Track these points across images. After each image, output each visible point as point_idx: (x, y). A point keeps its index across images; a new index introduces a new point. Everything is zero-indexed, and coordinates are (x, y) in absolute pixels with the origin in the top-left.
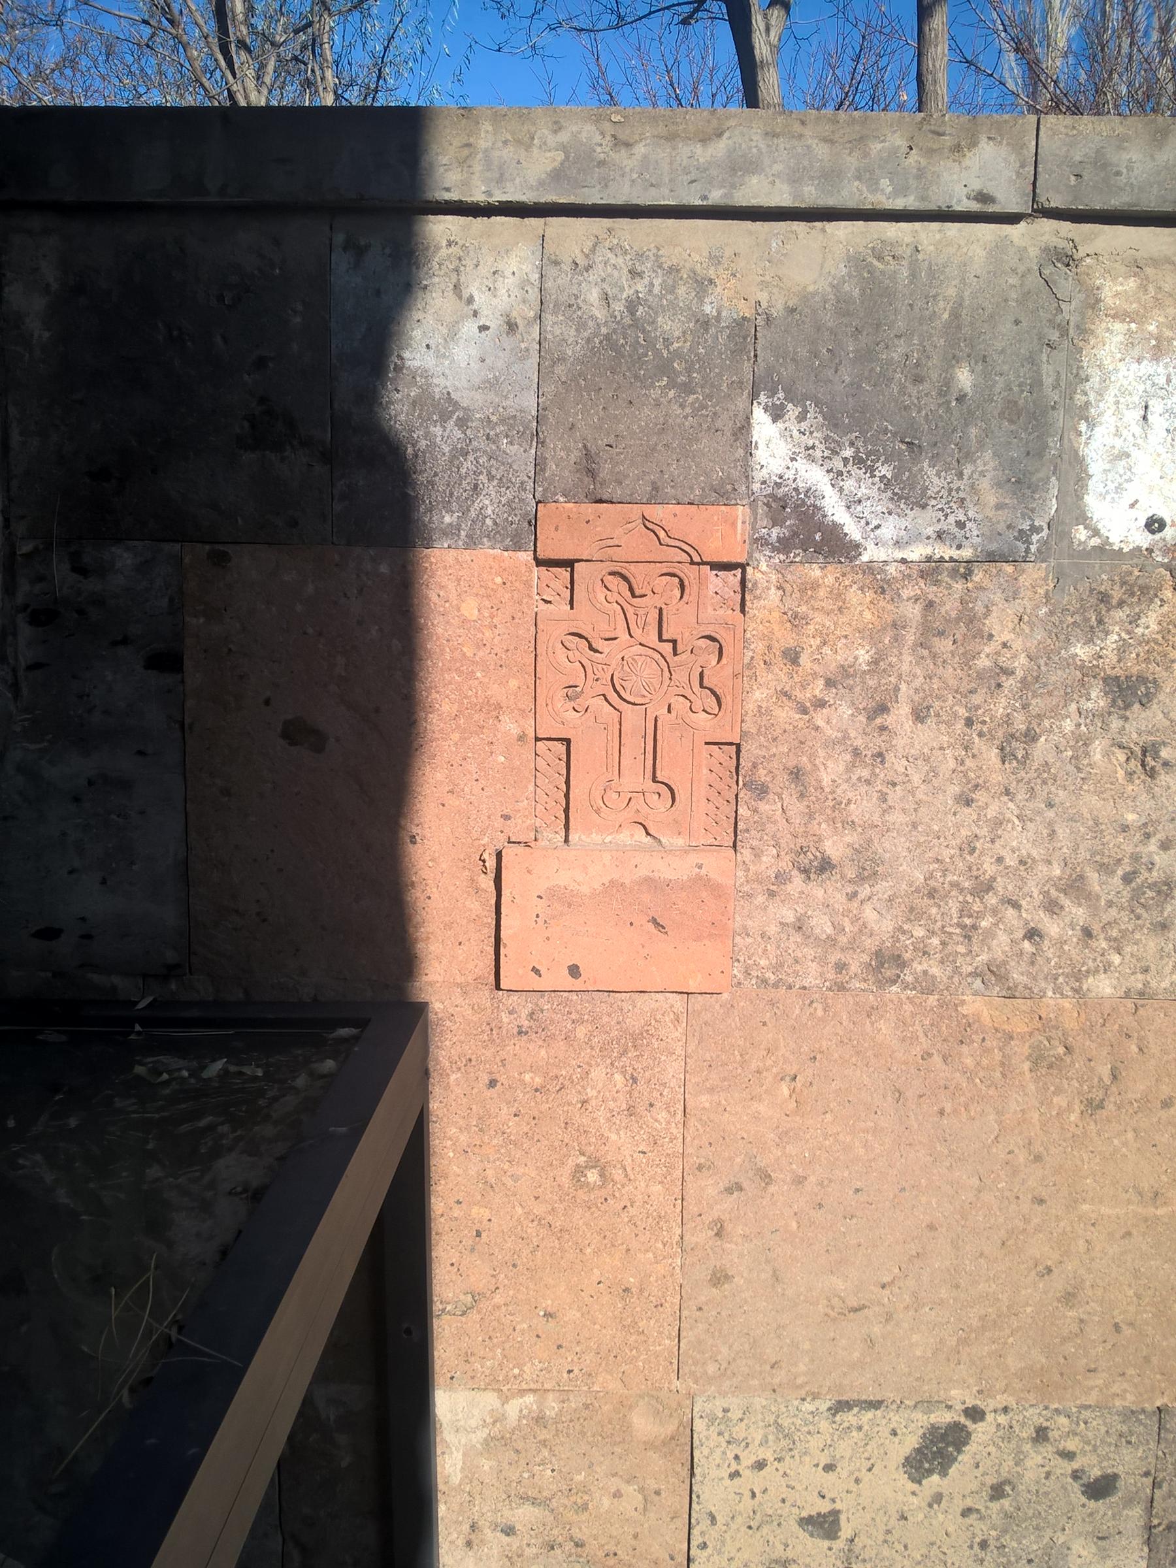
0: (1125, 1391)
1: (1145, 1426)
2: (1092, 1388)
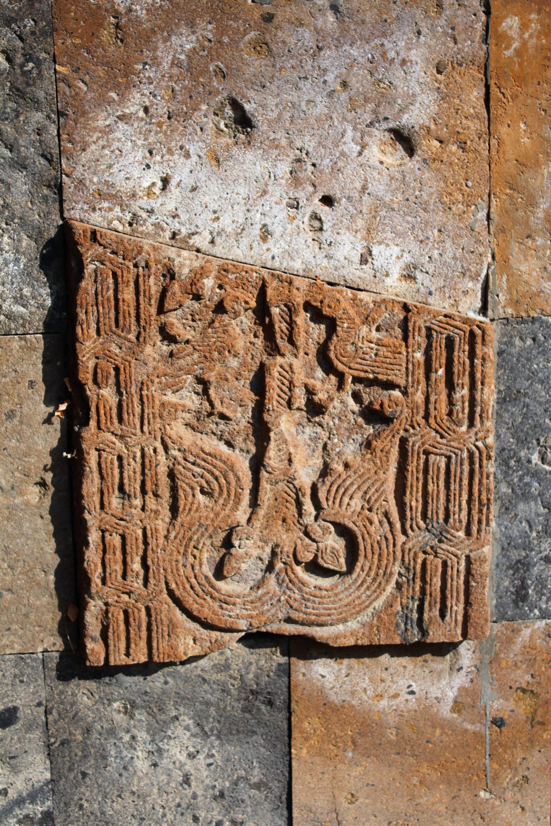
0: (12, 642)
1: (33, 668)
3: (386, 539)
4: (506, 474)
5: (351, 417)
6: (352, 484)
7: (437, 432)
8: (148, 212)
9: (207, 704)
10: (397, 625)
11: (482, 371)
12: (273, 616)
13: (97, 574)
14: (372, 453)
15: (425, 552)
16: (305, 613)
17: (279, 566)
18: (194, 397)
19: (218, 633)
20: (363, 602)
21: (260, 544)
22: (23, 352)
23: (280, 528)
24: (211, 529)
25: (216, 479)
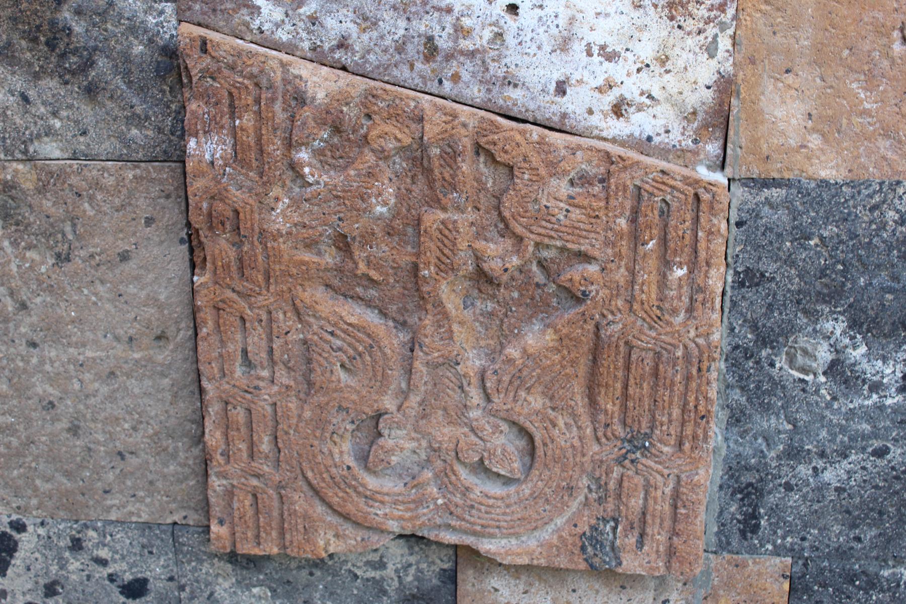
0: (139, 510)
1: (162, 540)
12: (429, 520)
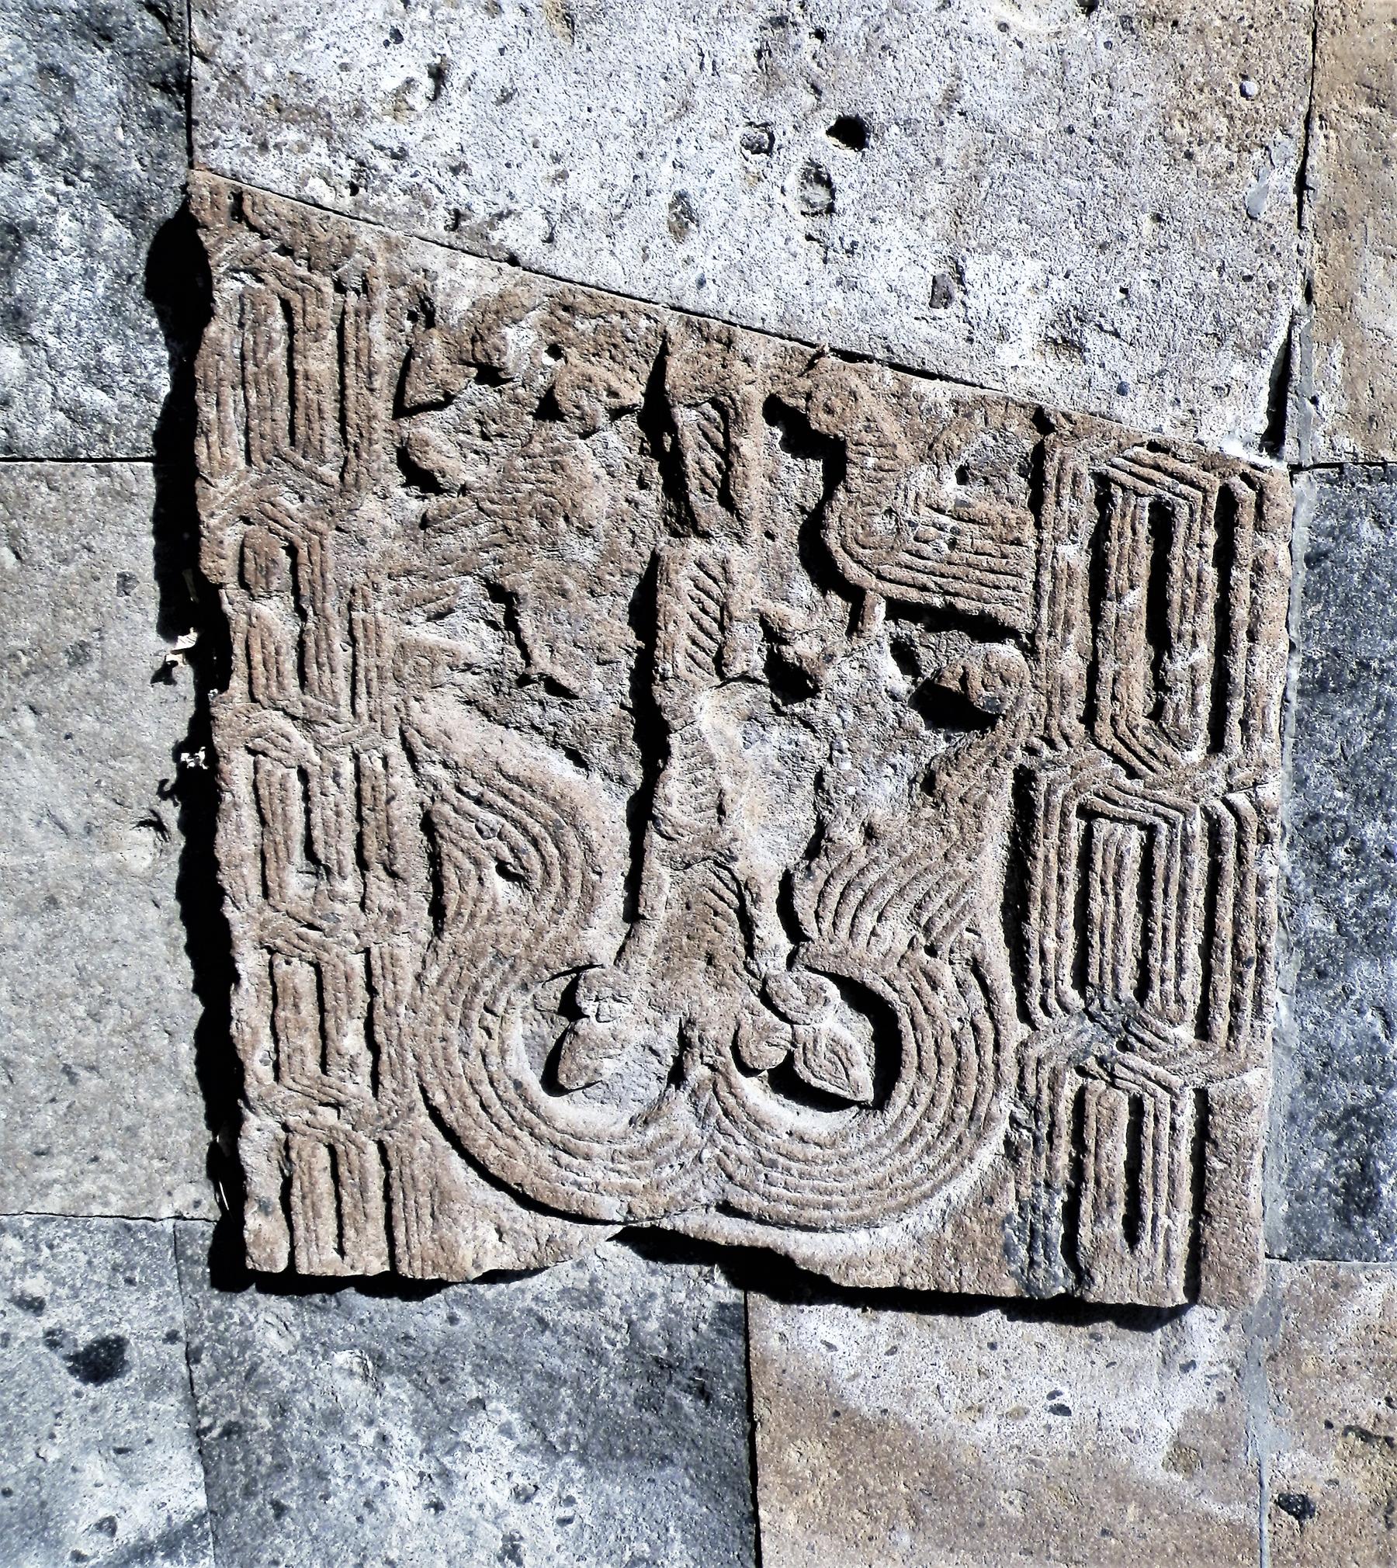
2: (49, 1184)
3: (976, 1028)
4: (1321, 883)
5: (887, 707)
6: (883, 881)
7: (1117, 759)
8: (394, 156)
9: (553, 1378)
10: (1008, 1250)
11: (1254, 601)
12: (685, 1194)
13: (259, 1054)
14: (936, 806)
15: (1082, 1071)
16: (767, 1197)
17: (697, 1072)
18: (486, 632)
19: (556, 1222)
20: (916, 1184)
21: (651, 1014)
22: (105, 503)
23: (700, 978)
24: (524, 969)
25: (535, 842)
